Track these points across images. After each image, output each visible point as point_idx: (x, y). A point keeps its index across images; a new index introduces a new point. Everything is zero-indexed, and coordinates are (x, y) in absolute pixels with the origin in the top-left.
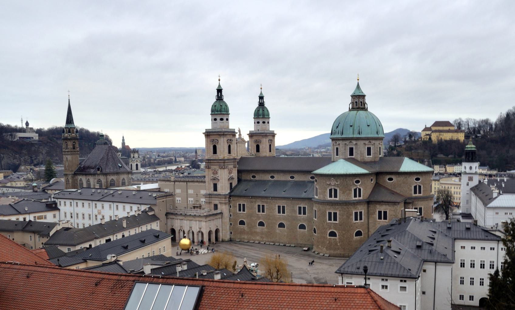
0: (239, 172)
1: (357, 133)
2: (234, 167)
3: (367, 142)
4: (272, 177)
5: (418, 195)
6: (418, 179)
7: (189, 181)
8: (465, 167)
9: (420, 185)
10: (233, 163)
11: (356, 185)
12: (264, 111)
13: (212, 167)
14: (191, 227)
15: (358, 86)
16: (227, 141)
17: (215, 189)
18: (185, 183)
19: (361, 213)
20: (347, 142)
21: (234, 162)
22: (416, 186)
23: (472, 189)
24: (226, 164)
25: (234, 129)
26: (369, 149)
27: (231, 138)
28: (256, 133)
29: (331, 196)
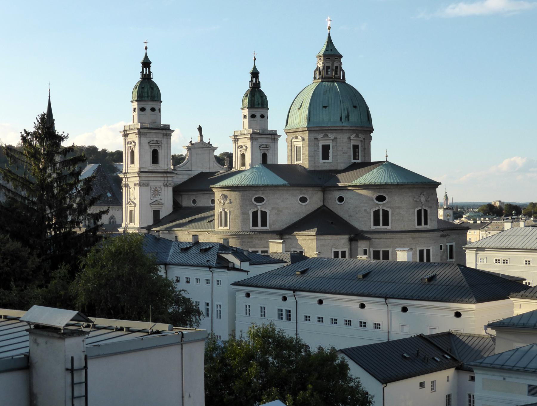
1: (303, 121)
2: (164, 186)
3: (320, 136)
5: (381, 227)
6: (381, 199)
9: (385, 209)
10: (162, 179)
11: (257, 206)
12: (254, 96)
15: (330, 41)
16: (149, 143)
21: (161, 177)
22: (378, 211)
24: (143, 179)
25: (169, 125)
26: (326, 148)
27: (160, 139)
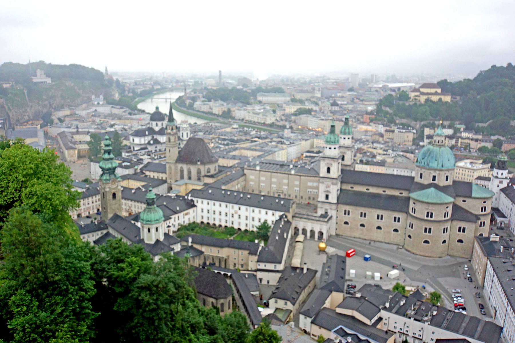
0: (342, 183)
4: (368, 190)
5: (483, 213)
6: (485, 202)
7: (273, 172)
8: (497, 173)
13: (325, 183)
14: (313, 228)
17: (327, 197)
18: (270, 173)
19: (447, 228)
20: (432, 172)
23: (502, 190)
26: (447, 177)
28: (342, 147)
29: (427, 216)
